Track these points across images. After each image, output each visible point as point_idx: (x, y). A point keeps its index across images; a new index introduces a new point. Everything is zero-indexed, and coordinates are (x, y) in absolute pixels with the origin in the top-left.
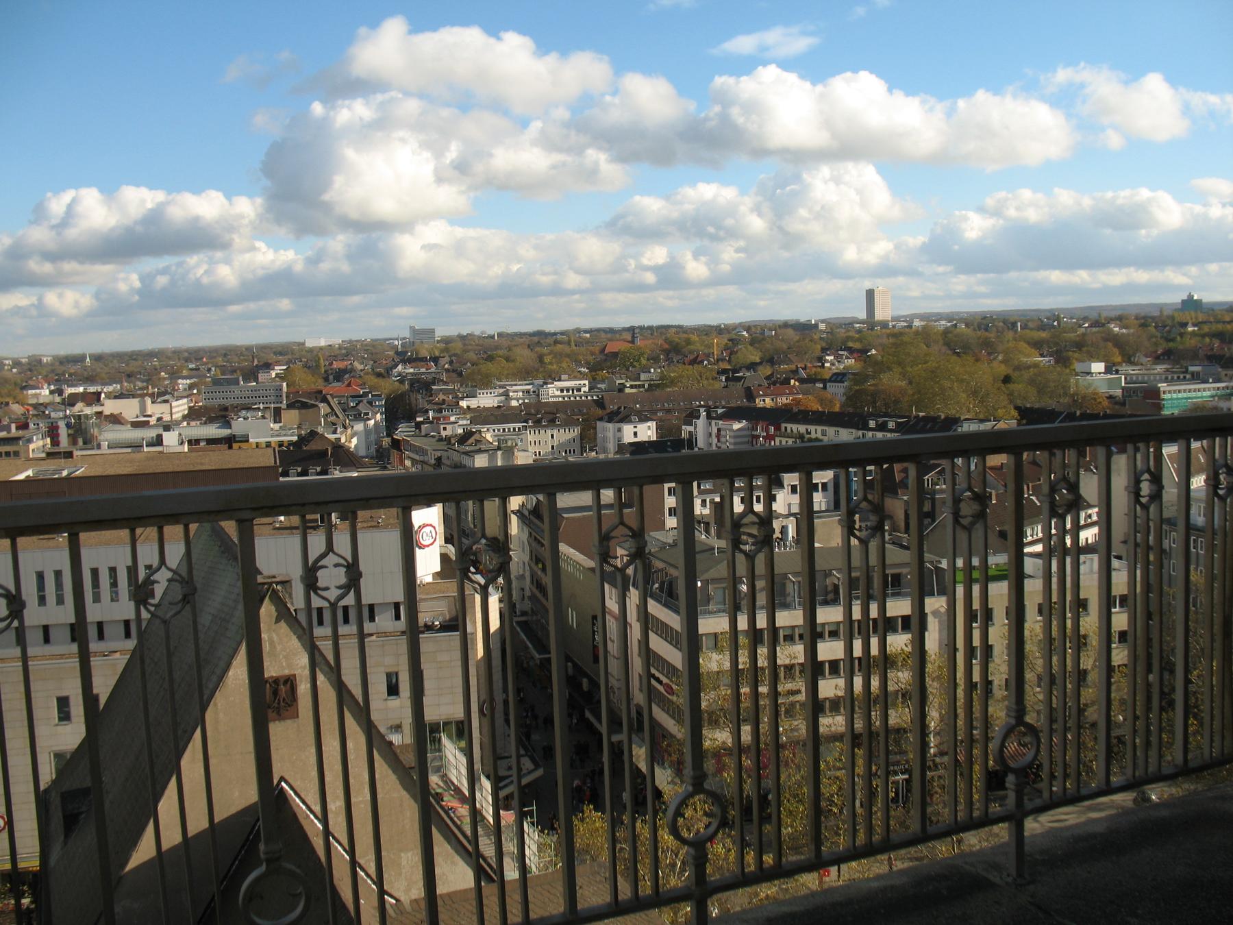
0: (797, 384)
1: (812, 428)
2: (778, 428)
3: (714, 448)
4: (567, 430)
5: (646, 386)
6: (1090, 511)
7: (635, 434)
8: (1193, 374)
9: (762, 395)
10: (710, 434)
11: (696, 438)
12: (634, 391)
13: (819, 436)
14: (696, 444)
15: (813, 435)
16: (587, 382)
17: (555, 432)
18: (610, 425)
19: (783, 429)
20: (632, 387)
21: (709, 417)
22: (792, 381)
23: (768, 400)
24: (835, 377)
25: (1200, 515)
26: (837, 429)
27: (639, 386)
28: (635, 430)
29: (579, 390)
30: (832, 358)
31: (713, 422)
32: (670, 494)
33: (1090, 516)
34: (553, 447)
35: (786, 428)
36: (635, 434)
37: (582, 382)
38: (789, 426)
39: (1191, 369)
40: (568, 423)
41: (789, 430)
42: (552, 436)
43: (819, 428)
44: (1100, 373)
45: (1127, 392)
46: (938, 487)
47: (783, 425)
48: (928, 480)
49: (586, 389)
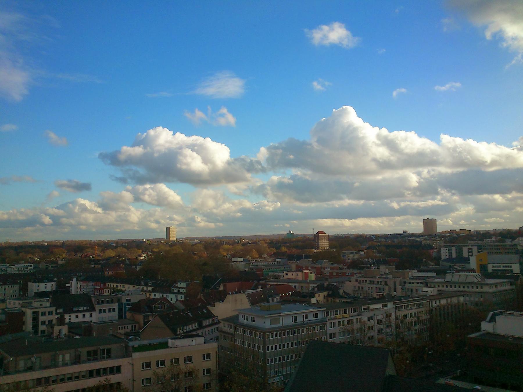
0: (123, 266)
1: (119, 285)
2: (105, 285)
3: (79, 293)
4: (13, 286)
5: (59, 266)
6: (213, 318)
7: (46, 288)
8: (278, 261)
9: (108, 271)
10: (77, 287)
11: (71, 289)
12: (52, 269)
13: (121, 288)
14: (71, 292)
15: (119, 288)
16: (32, 265)
17: (7, 287)
18: (34, 284)
19: (107, 286)
20: (52, 267)
21: (77, 280)
22: (121, 265)
23: (110, 273)
24: (140, 263)
25: (245, 320)
26: (129, 285)
27: (56, 267)
28: (46, 286)
29: (27, 268)
30: (145, 255)
31: (79, 282)
32: (42, 315)
33: (213, 320)
34: (5, 295)
35: (108, 285)
36: (46, 288)
37: (30, 265)
38: (109, 284)
39: (277, 260)
40: (14, 283)
41: (110, 286)
42: (5, 289)
43: (122, 285)
44: (241, 262)
45: (250, 269)
46: (158, 309)
47: (107, 284)
48: (154, 306)
49: (32, 268)
